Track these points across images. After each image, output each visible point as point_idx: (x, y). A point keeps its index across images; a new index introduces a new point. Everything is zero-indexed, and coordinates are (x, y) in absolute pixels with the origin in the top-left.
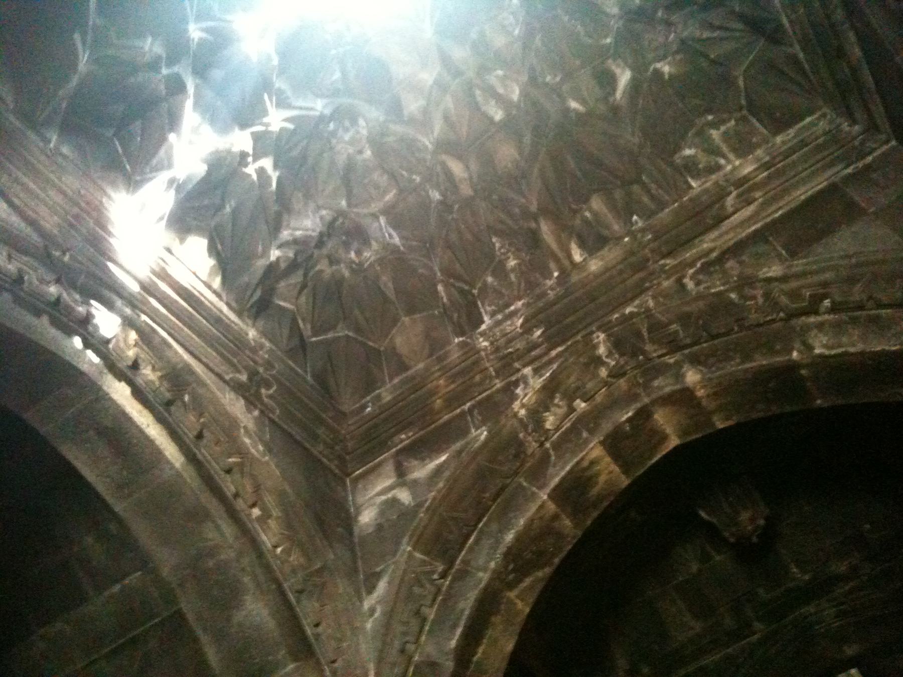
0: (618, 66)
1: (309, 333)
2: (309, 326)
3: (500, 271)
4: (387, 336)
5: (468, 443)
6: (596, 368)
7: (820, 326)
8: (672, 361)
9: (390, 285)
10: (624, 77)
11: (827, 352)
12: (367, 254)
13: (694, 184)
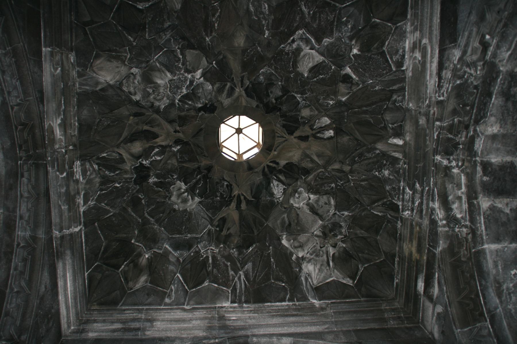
1: (351, 281)
2: (348, 279)
3: (386, 181)
4: (380, 252)
6: (450, 171)
8: (472, 133)
9: (363, 232)
10: (348, 70)
11: (509, 53)
12: (343, 231)
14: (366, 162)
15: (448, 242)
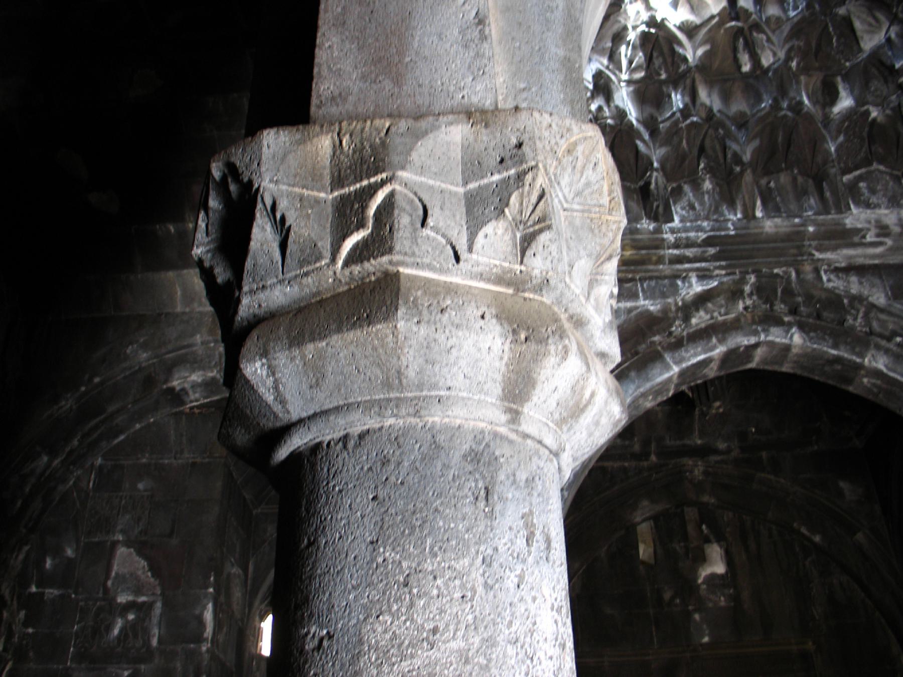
0: (845, 89)
5: (636, 308)
7: (887, 351)
11: (885, 370)
13: (852, 206)
14: (718, 147)
15: (660, 315)
